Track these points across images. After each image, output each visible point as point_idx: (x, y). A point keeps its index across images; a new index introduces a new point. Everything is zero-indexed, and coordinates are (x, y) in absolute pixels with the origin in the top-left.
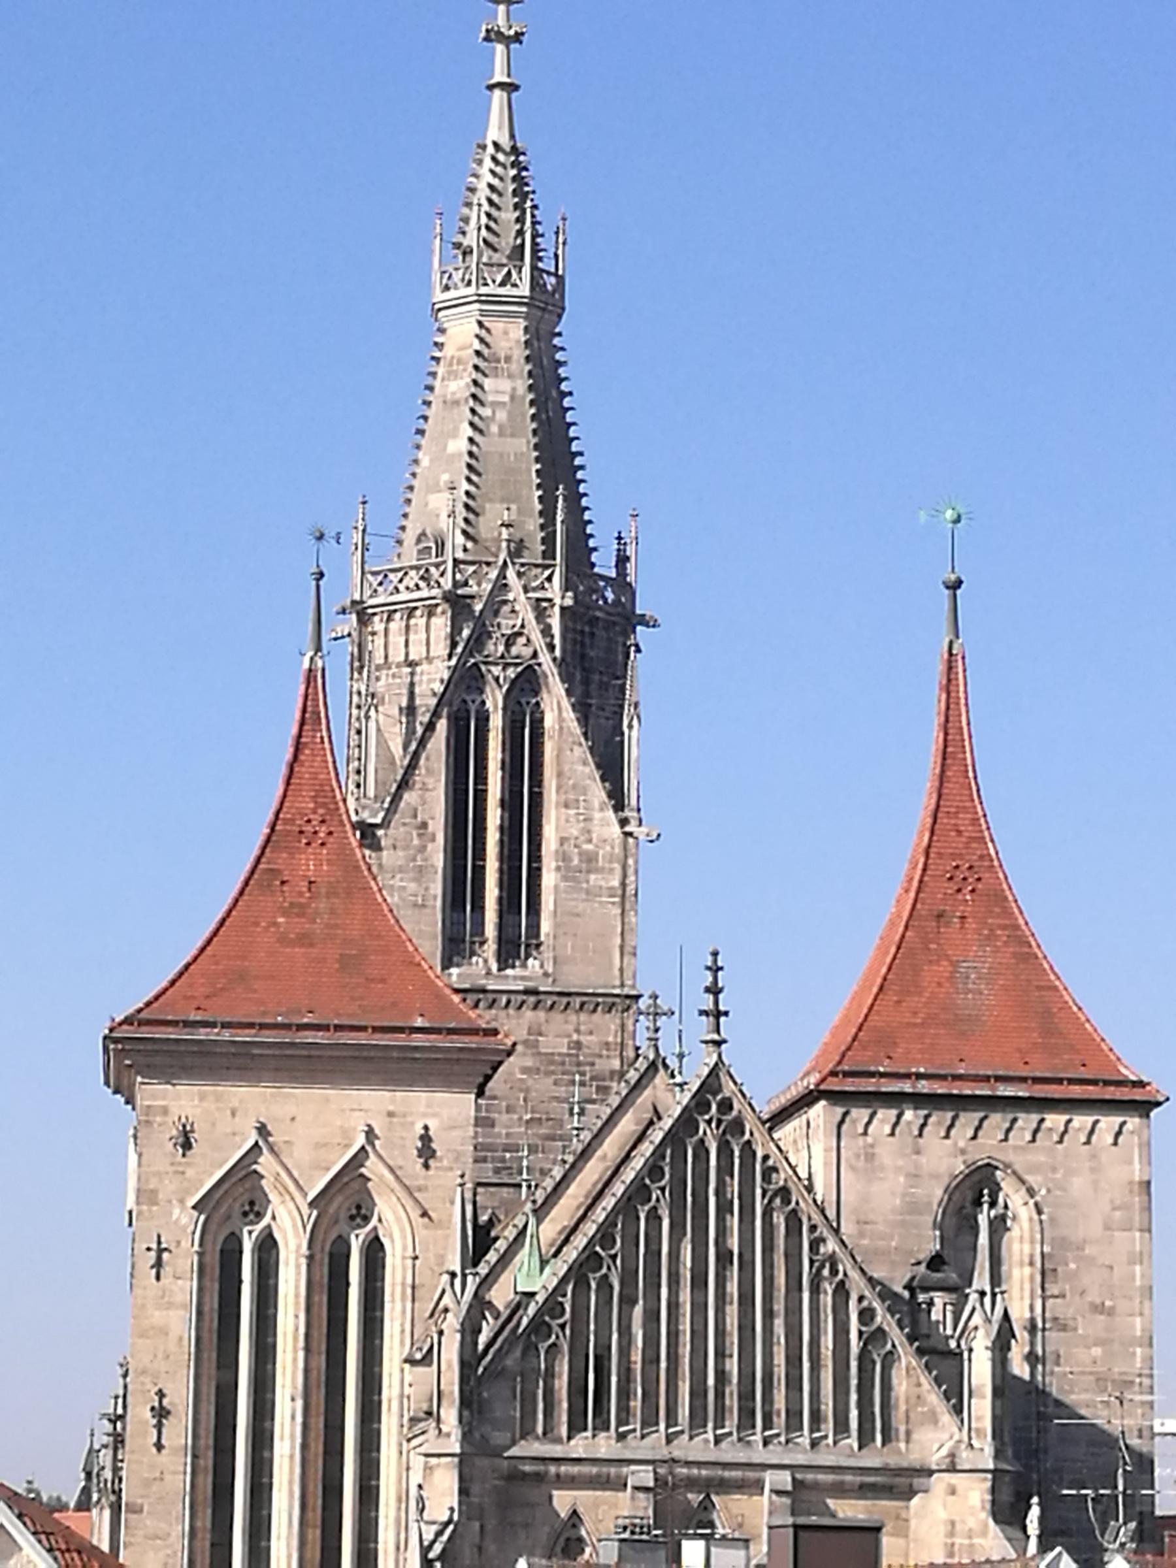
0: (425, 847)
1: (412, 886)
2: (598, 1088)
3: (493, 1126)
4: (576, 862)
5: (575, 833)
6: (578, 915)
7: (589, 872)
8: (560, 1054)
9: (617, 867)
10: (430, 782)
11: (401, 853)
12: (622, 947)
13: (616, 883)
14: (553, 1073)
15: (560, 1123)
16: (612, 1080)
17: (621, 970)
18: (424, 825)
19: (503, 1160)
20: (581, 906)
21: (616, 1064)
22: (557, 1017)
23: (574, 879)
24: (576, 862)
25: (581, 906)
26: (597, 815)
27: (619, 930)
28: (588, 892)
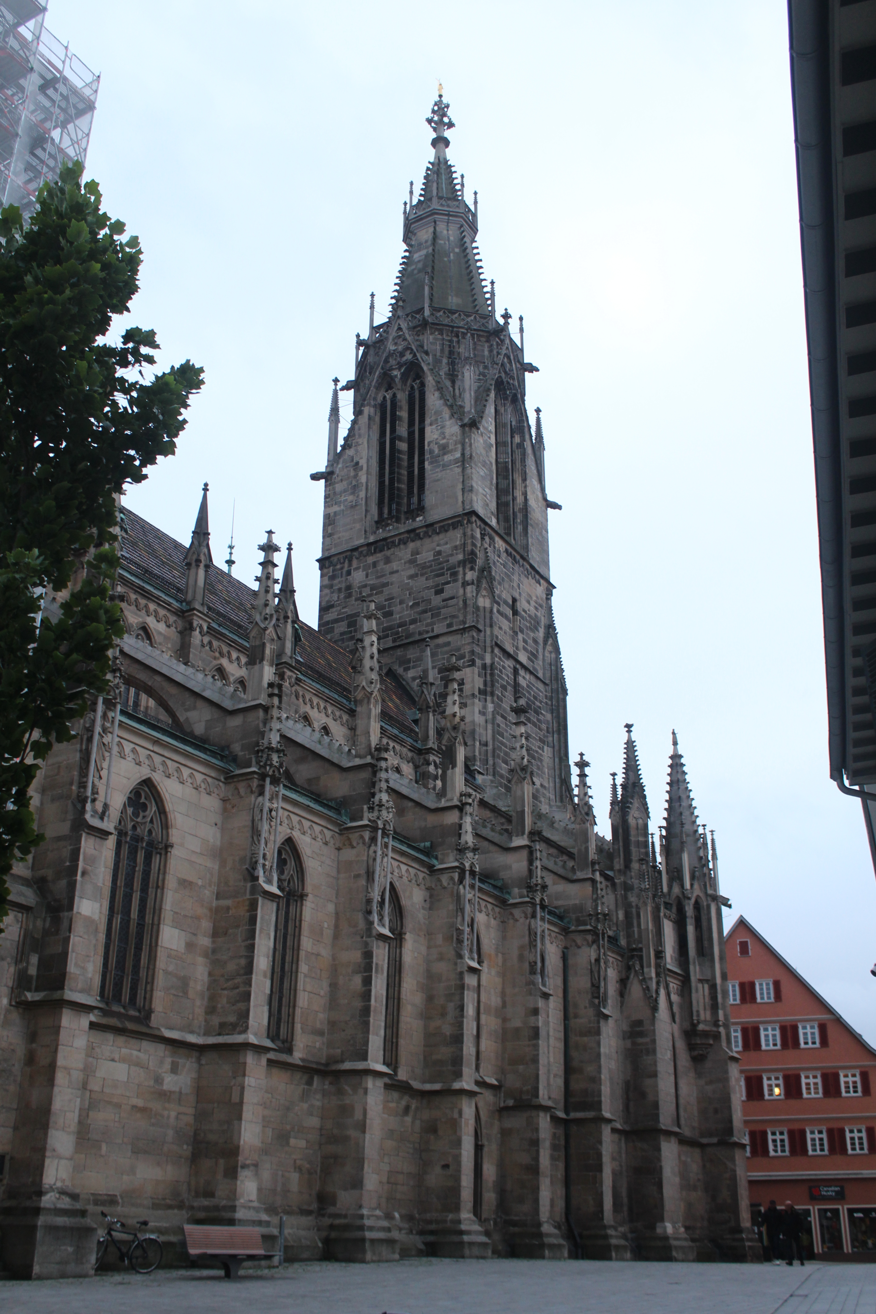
0: (356, 476)
1: (350, 498)
3: (392, 615)
4: (436, 451)
5: (436, 437)
6: (438, 480)
7: (444, 454)
8: (429, 562)
9: (459, 446)
10: (360, 441)
11: (345, 483)
12: (463, 490)
13: (458, 455)
14: (426, 573)
15: (429, 601)
16: (459, 566)
17: (463, 502)
18: (357, 463)
20: (440, 475)
21: (460, 557)
22: (427, 541)
23: (436, 461)
24: (436, 451)
25: (440, 475)
28: (444, 466)
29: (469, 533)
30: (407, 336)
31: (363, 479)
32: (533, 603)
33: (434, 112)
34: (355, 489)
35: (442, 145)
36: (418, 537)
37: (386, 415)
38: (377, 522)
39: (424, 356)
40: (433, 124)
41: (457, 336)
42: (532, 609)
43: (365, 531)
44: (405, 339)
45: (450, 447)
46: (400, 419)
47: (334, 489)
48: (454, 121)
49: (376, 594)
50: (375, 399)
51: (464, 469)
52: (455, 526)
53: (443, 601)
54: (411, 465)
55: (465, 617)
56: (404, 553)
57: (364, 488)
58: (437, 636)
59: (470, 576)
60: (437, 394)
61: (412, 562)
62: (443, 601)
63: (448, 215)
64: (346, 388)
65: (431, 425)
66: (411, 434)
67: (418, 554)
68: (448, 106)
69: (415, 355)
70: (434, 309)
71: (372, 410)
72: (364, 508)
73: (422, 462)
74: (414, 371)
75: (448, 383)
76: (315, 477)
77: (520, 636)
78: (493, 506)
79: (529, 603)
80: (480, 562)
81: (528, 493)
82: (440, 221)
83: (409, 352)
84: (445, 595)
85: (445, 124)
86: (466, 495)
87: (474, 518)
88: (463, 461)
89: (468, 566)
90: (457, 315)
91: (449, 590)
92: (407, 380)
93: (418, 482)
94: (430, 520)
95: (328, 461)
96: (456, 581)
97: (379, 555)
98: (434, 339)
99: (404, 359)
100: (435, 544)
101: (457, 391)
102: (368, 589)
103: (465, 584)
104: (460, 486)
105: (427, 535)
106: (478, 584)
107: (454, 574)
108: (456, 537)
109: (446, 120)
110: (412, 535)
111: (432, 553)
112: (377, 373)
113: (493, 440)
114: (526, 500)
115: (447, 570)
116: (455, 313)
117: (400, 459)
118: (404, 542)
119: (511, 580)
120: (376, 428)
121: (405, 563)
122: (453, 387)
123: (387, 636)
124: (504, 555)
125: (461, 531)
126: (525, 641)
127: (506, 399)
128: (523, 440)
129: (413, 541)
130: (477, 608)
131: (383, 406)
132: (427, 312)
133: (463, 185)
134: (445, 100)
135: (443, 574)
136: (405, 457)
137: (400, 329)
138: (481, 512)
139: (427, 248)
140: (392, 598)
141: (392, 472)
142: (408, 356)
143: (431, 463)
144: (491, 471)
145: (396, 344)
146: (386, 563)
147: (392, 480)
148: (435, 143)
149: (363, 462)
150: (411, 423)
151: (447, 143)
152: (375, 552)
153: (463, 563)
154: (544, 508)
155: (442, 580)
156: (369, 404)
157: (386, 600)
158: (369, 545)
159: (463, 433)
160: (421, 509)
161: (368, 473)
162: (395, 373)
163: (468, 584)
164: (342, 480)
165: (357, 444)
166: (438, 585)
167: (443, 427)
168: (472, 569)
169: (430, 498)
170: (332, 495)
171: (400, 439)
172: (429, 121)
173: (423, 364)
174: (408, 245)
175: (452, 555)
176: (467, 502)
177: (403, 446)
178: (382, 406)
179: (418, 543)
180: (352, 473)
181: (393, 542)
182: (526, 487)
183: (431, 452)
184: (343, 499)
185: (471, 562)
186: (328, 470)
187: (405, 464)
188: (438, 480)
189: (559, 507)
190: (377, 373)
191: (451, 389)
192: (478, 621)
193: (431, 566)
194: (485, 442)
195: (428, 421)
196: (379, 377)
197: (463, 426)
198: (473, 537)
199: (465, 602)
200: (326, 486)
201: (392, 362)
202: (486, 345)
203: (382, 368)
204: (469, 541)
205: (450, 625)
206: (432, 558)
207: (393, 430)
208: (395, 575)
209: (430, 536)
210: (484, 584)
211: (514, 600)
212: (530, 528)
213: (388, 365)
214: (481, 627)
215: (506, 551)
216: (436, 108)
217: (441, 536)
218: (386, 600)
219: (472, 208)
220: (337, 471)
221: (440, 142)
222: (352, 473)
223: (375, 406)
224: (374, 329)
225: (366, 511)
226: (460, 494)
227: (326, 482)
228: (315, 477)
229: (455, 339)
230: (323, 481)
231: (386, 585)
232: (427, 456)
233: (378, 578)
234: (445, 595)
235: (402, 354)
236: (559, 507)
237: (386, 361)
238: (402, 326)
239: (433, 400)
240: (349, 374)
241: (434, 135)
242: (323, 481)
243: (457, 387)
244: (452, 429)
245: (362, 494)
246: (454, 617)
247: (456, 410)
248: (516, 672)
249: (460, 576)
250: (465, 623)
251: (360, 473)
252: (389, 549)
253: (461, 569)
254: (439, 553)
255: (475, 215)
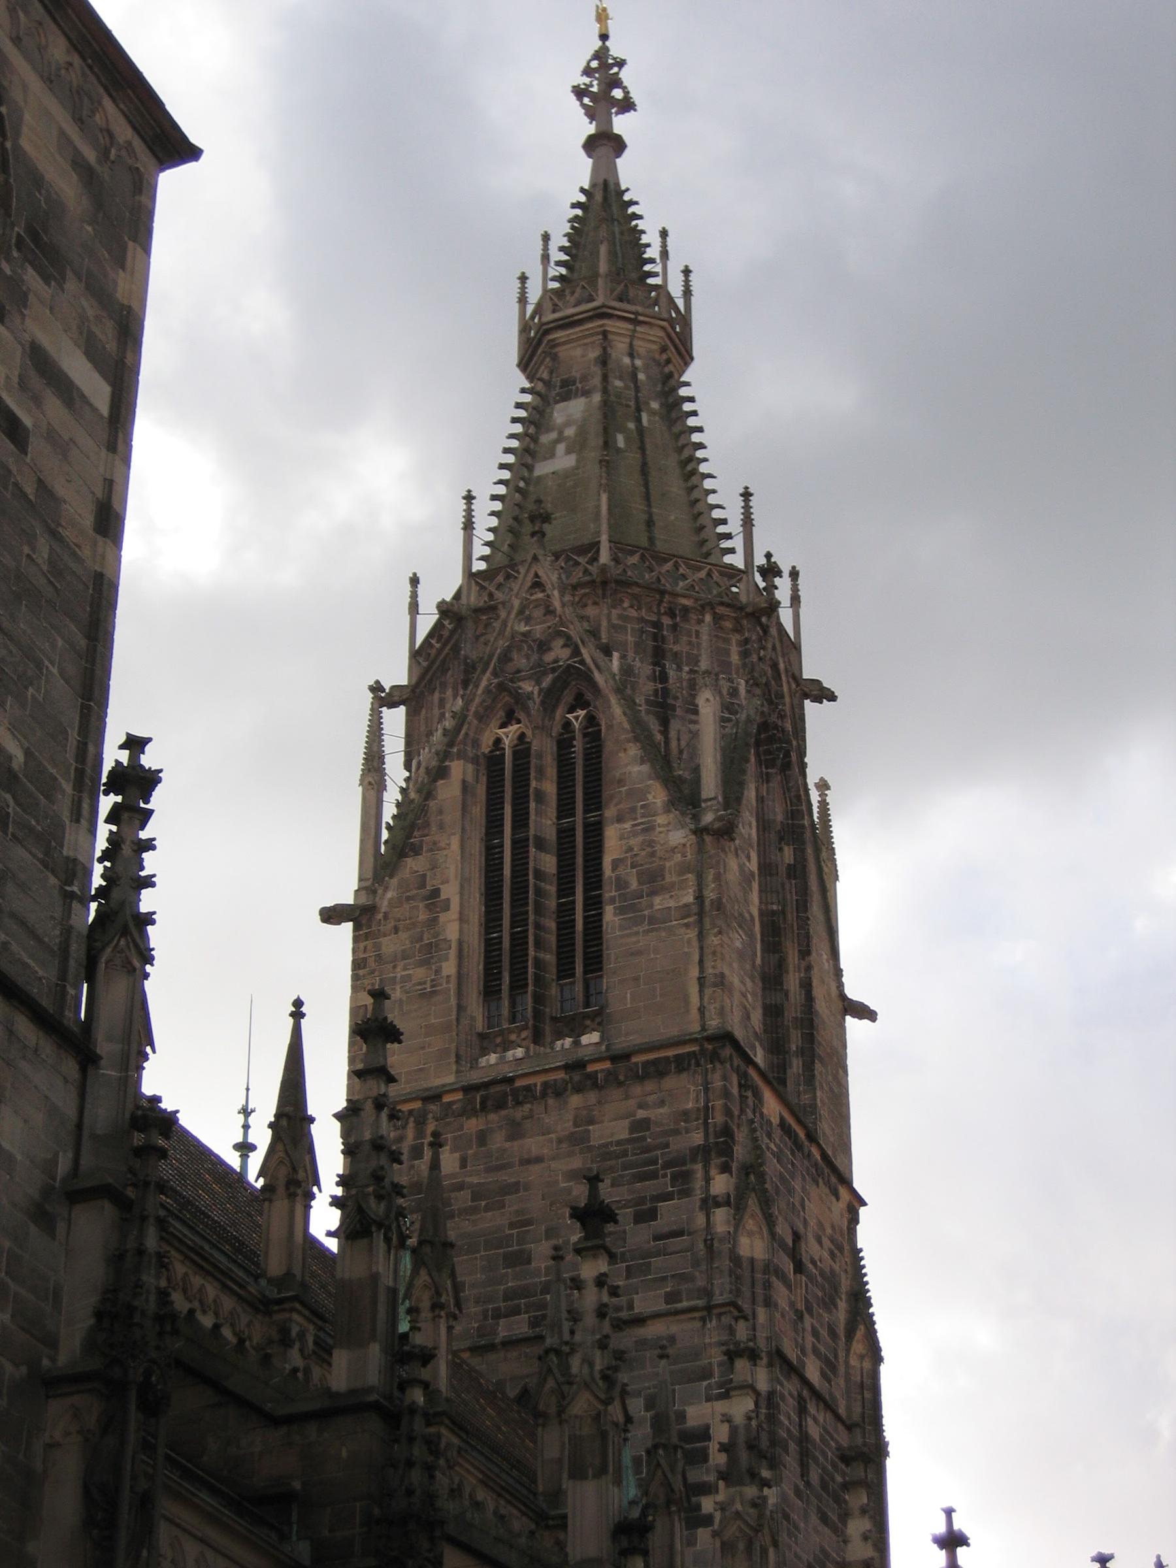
0: (434, 921)
1: (419, 973)
2: (674, 1178)
3: (529, 1262)
4: (634, 885)
6: (639, 953)
7: (653, 893)
8: (619, 1143)
11: (403, 935)
12: (701, 981)
13: (690, 899)
16: (694, 1160)
17: (702, 1010)
18: (436, 893)
19: (543, 1306)
21: (697, 1138)
22: (616, 1093)
23: (633, 908)
24: (634, 885)
26: (661, 820)
27: (696, 958)
28: (652, 920)
29: (718, 1084)
30: (557, 604)
31: (452, 932)
32: (826, 1242)
33: (588, 71)
34: (430, 952)
35: (604, 150)
36: (592, 1083)
37: (504, 783)
38: (482, 1036)
39: (599, 655)
40: (586, 100)
41: (671, 613)
42: (826, 1255)
43: (458, 1057)
44: (550, 611)
45: (670, 878)
46: (540, 796)
47: (377, 947)
48: (635, 96)
49: (487, 1209)
50: (476, 743)
51: (701, 936)
52: (681, 1064)
53: (657, 1238)
54: (565, 913)
55: (710, 1279)
56: (559, 1118)
57: (453, 953)
58: (640, 1321)
59: (721, 1184)
60: (634, 750)
61: (577, 1140)
62: (657, 1238)
63: (635, 322)
64: (392, 705)
65: (620, 819)
66: (565, 834)
67: (591, 1122)
68: (621, 63)
69: (576, 652)
70: (620, 548)
71: (470, 768)
72: (453, 1001)
73: (594, 904)
74: (573, 685)
75: (654, 725)
76: (331, 915)
77: (808, 1321)
78: (757, 1017)
79: (820, 1243)
80: (740, 1152)
81: (815, 983)
82: (604, 324)
83: (561, 642)
84: (662, 1223)
85: (614, 102)
86: (708, 991)
87: (727, 1051)
88: (701, 914)
89: (716, 1161)
90: (669, 566)
91: (670, 1214)
92: (553, 711)
93: (584, 952)
94: (622, 1043)
95: (360, 880)
96: (686, 1193)
97: (493, 1117)
98: (620, 617)
99: (549, 657)
100: (632, 1103)
101: (674, 744)
102: (466, 1195)
103: (709, 1203)
104: (695, 972)
105: (612, 1079)
106: (736, 1203)
107: (683, 1178)
108: (685, 1091)
109: (618, 94)
110: (577, 1077)
111: (626, 1123)
112: (484, 683)
113: (753, 866)
114: (810, 998)
115: (663, 1168)
116: (666, 561)
117: (539, 892)
118: (557, 1091)
119: (791, 1191)
120: (478, 810)
121: (560, 1141)
122: (665, 732)
123: (516, 1311)
124: (777, 1133)
125: (699, 1079)
126: (815, 1333)
127: (770, 764)
128: (800, 852)
129: (578, 1090)
130: (736, 1259)
131: (494, 762)
132: (604, 557)
133: (665, 254)
134: (616, 49)
135: (653, 1176)
136: (551, 889)
137: (538, 585)
138: (739, 1034)
139: (586, 393)
140: (528, 1223)
141: (519, 919)
142: (559, 653)
143: (620, 911)
144: (751, 936)
145: (528, 620)
146: (511, 1137)
147: (519, 942)
148: (591, 145)
149: (450, 891)
150: (565, 807)
151: (618, 145)
152: (484, 1108)
153: (703, 1153)
154: (839, 1017)
155: (650, 1188)
156: (461, 755)
157: (512, 1225)
158: (468, 1089)
159: (701, 849)
160: (598, 1018)
161: (462, 919)
162: (527, 687)
163: (718, 1205)
164: (396, 930)
165: (435, 847)
166: (641, 1201)
167: (649, 829)
168: (725, 1169)
169: (619, 992)
170: (372, 963)
171: (541, 844)
172: (579, 92)
173: (596, 674)
174: (530, 378)
175: (676, 1132)
176: (712, 1010)
177: (549, 863)
178: (494, 762)
179: (592, 1097)
180: (423, 916)
181: (528, 1089)
182: (809, 968)
183: (621, 884)
184: (400, 973)
185: (721, 1153)
186: (363, 900)
187: (552, 903)
188: (639, 953)
189: (871, 1015)
190: (484, 683)
191: (659, 737)
192: (738, 1292)
193: (625, 1153)
194: (741, 867)
195: (610, 812)
196: (487, 691)
197: (699, 832)
198: (726, 1094)
199: (709, 1245)
200: (356, 939)
201: (520, 661)
202: (735, 638)
203: (495, 674)
204: (719, 1103)
205: (671, 1298)
206: (625, 1135)
207: (521, 820)
208: (536, 1168)
209: (620, 1084)
210: (753, 1204)
211: (797, 1237)
212: (818, 1065)
213: (510, 667)
214: (746, 1306)
215: (783, 1124)
216: (595, 64)
217: (650, 1086)
218: (512, 1225)
219: (680, 303)
220: (384, 906)
221: (605, 145)
222: (423, 916)
223: (475, 761)
224: (470, 576)
225: (460, 1008)
226: (694, 990)
227: (356, 929)
228: (331, 915)
229: (666, 621)
230: (349, 926)
231: (515, 1188)
232: (609, 893)
233: (489, 1170)
234: (662, 1223)
235: (543, 646)
236: (871, 1015)
237: (505, 658)
238: (544, 578)
239: (628, 765)
240: (397, 674)
241: (591, 129)
242: (349, 926)
243: (673, 734)
244: (676, 836)
245: (449, 968)
246: (683, 1278)
247: (685, 798)
248: (802, 1410)
249: (698, 1184)
250: (708, 1293)
251: (443, 917)
252: (518, 1103)
253: (699, 1167)
254: (642, 1125)
255: (685, 320)
